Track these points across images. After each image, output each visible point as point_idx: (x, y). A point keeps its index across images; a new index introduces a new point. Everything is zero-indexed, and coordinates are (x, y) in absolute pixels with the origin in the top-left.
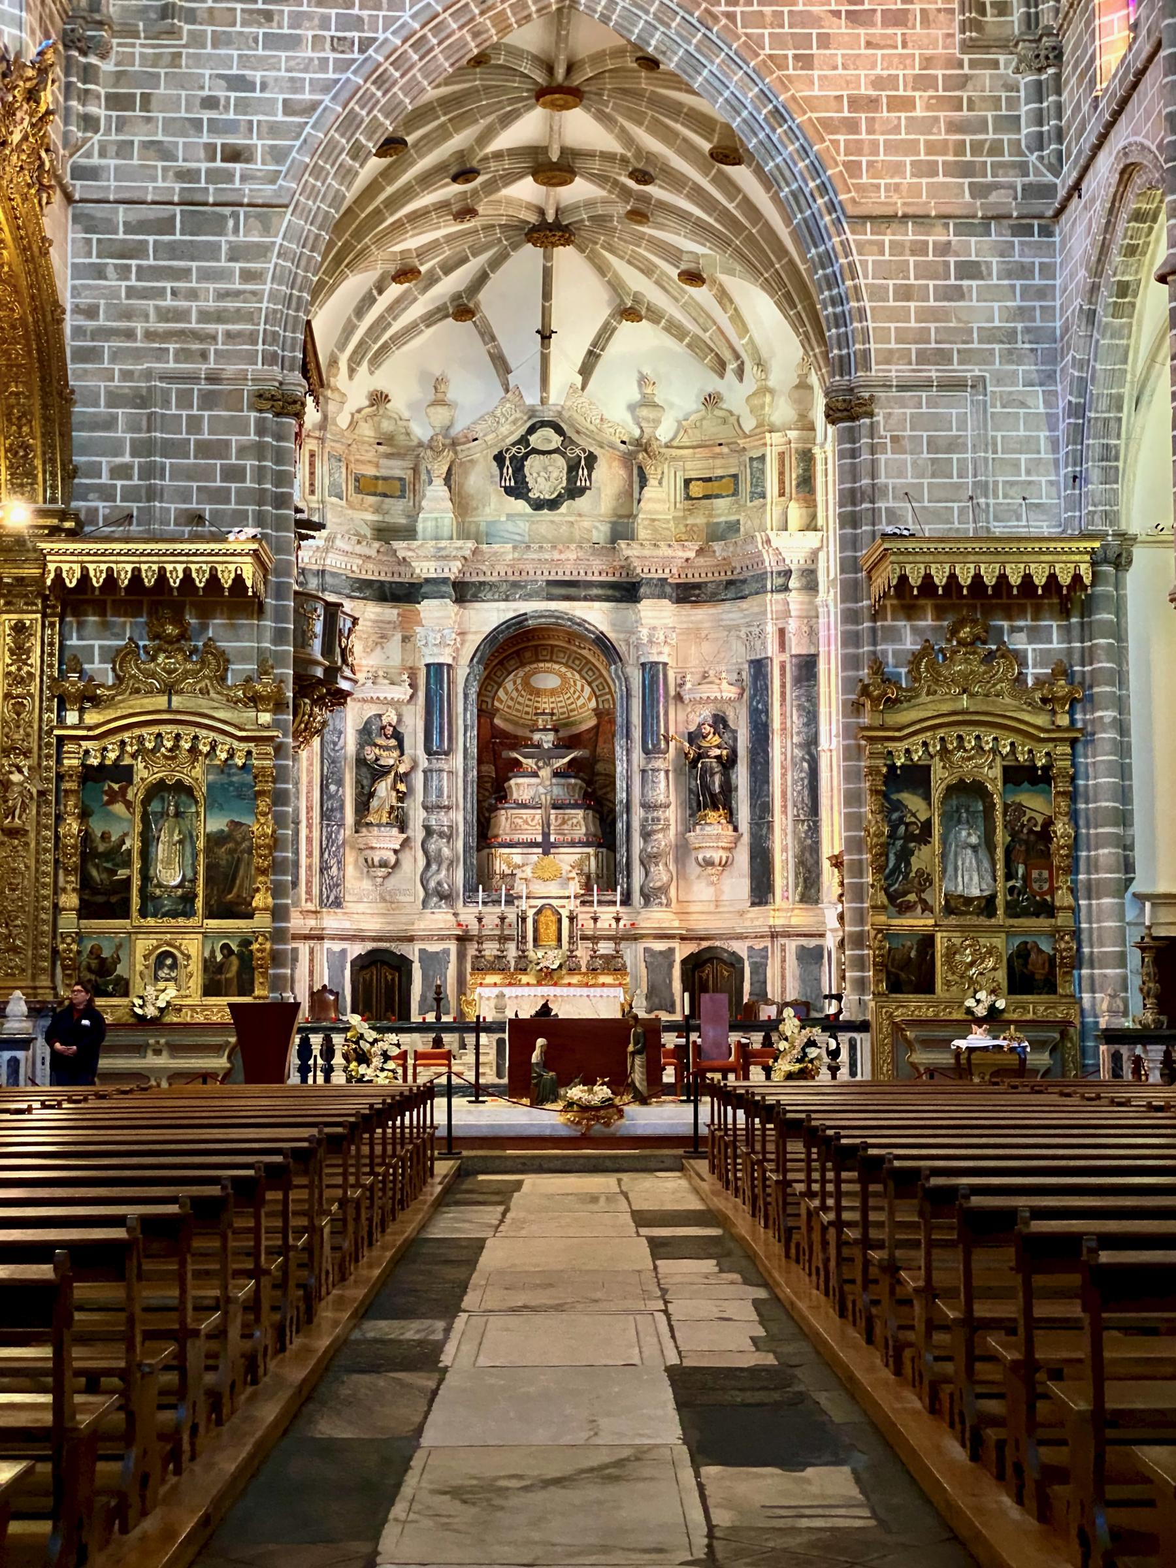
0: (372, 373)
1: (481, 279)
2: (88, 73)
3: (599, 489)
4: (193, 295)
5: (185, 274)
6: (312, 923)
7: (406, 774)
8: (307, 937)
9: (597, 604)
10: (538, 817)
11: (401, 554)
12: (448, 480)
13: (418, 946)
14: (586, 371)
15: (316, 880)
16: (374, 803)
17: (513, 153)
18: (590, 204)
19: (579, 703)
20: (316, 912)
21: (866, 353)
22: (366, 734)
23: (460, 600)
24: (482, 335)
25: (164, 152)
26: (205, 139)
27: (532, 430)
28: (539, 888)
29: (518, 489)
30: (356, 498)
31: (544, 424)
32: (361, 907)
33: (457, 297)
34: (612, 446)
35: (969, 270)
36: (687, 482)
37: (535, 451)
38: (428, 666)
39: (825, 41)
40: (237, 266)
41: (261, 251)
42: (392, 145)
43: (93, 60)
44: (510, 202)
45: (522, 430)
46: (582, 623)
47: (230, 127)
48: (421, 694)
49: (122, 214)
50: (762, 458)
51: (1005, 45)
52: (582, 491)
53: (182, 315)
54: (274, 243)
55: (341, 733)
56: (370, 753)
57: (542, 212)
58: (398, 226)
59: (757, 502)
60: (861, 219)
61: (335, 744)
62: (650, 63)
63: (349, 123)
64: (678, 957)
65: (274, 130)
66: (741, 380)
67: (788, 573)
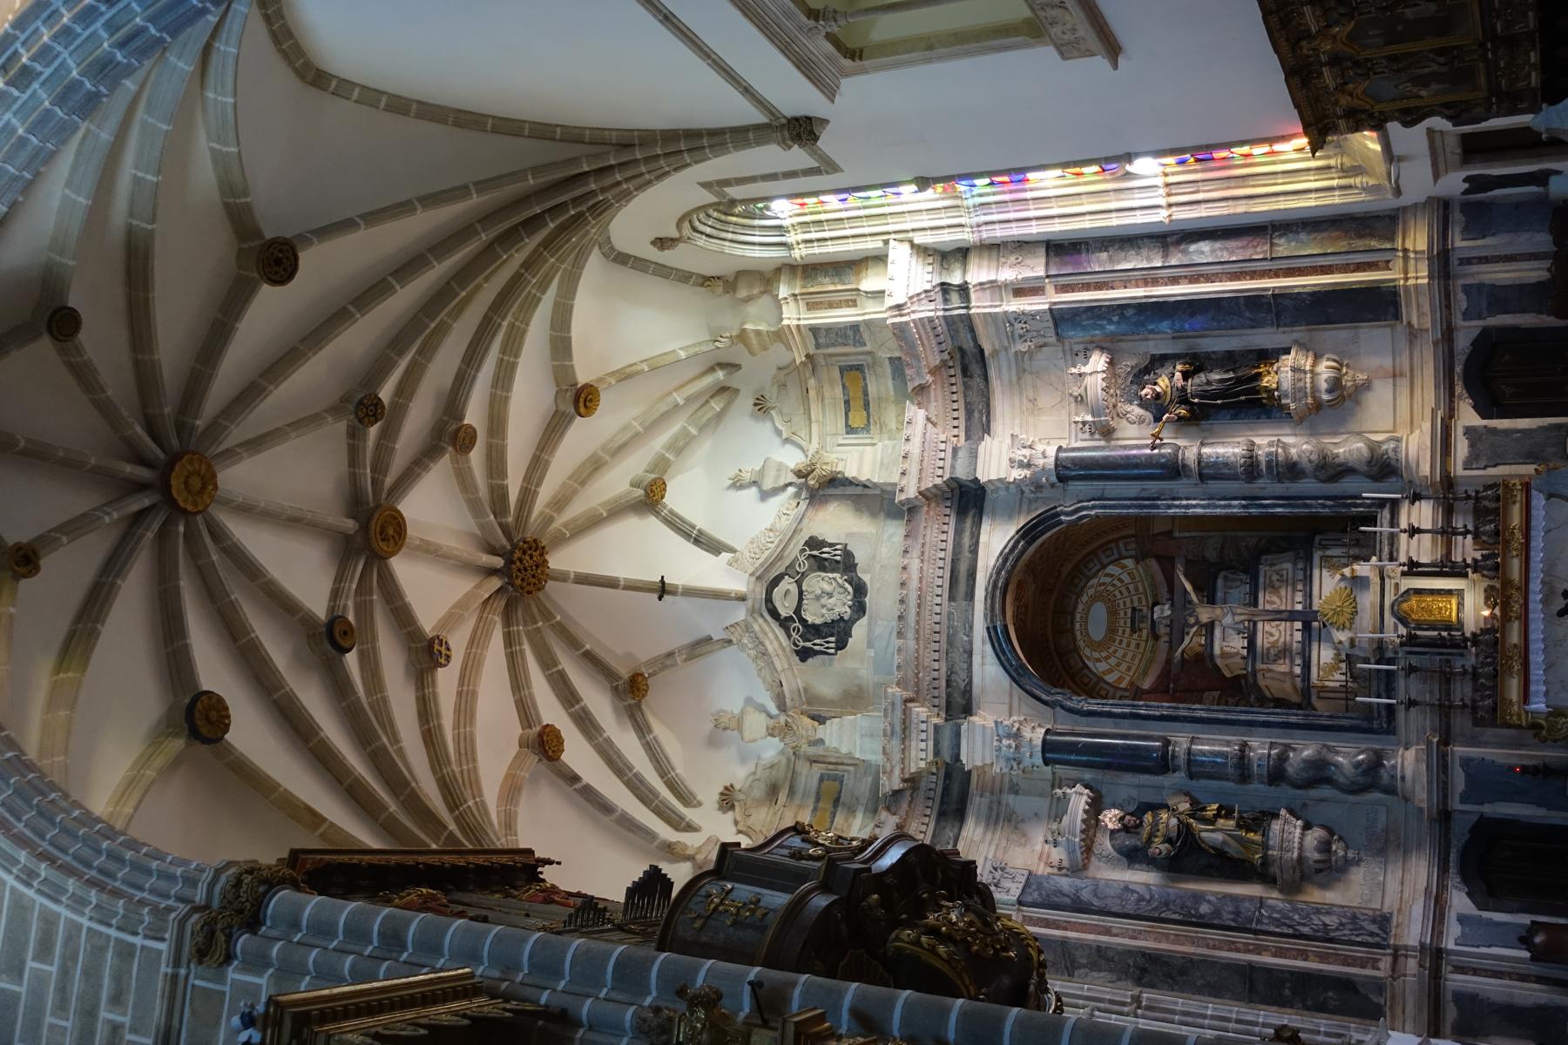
0: (700, 804)
1: (594, 662)
3: (847, 535)
6: (1412, 965)
7: (1194, 802)
8: (1436, 976)
9: (983, 538)
10: (1267, 628)
11: (897, 784)
12: (821, 720)
13: (1456, 804)
14: (714, 547)
15: (1344, 950)
16: (1234, 850)
19: (1126, 578)
20: (1395, 957)
22: (1134, 856)
23: (968, 710)
24: (664, 667)
27: (774, 613)
28: (1367, 616)
29: (839, 631)
31: (769, 600)
32: (1393, 885)
33: (616, 691)
36: (850, 430)
37: (798, 611)
38: (1046, 762)
40: (30, 964)
45: (775, 625)
46: (1004, 557)
48: (1088, 775)
50: (814, 330)
52: (848, 555)
54: (13, 891)
55: (1127, 889)
56: (1160, 847)
57: (491, 572)
59: (866, 336)
61: (1141, 899)
64: (1475, 421)
66: (737, 367)
67: (945, 288)
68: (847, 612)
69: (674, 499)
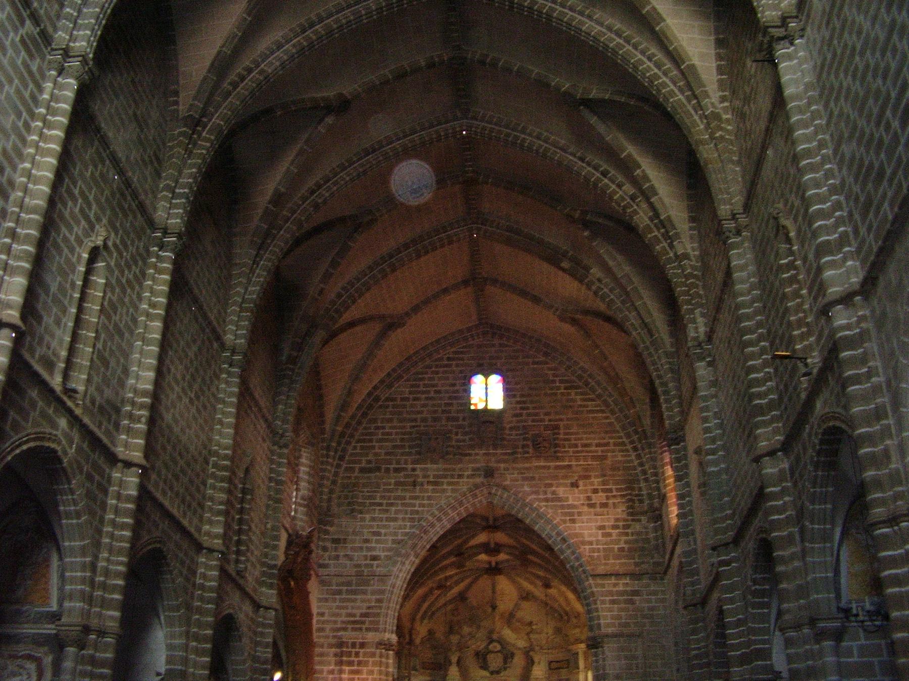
2: (327, 532)
4: (359, 608)
5: (355, 600)
17: (477, 546)
18: (507, 561)
21: (599, 624)
25: (350, 558)
26: (364, 553)
29: (485, 667)
30: (422, 671)
34: (520, 649)
35: (636, 593)
36: (550, 663)
37: (492, 652)
39: (579, 514)
41: (382, 592)
42: (434, 547)
43: (328, 528)
44: (478, 561)
47: (374, 549)
49: (335, 580)
50: (577, 653)
51: (644, 513)
53: (354, 615)
57: (490, 563)
58: (436, 573)
60: (594, 576)
62: (520, 521)
63: (414, 546)
65: (389, 550)
68: (491, 669)
69: (525, 605)
